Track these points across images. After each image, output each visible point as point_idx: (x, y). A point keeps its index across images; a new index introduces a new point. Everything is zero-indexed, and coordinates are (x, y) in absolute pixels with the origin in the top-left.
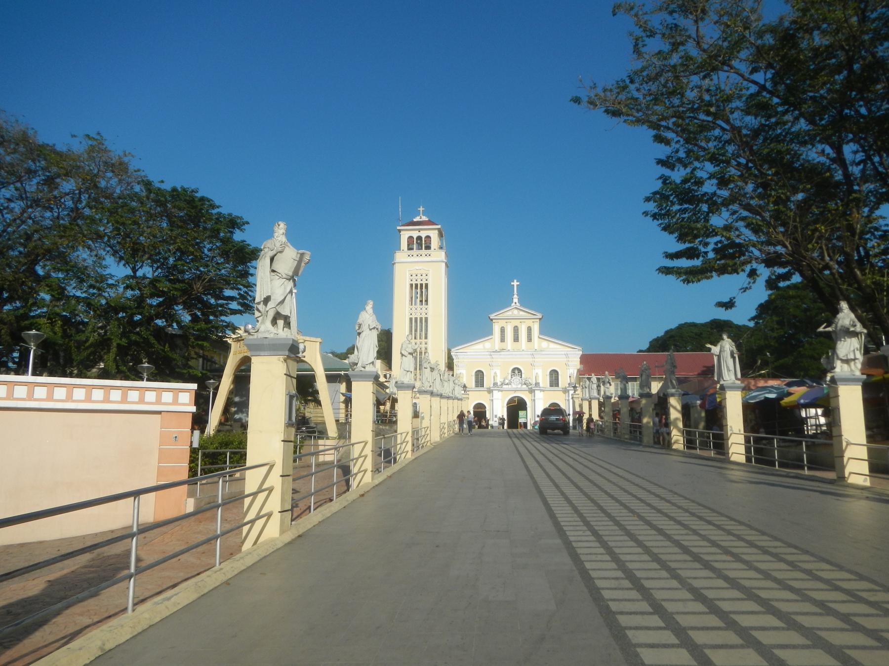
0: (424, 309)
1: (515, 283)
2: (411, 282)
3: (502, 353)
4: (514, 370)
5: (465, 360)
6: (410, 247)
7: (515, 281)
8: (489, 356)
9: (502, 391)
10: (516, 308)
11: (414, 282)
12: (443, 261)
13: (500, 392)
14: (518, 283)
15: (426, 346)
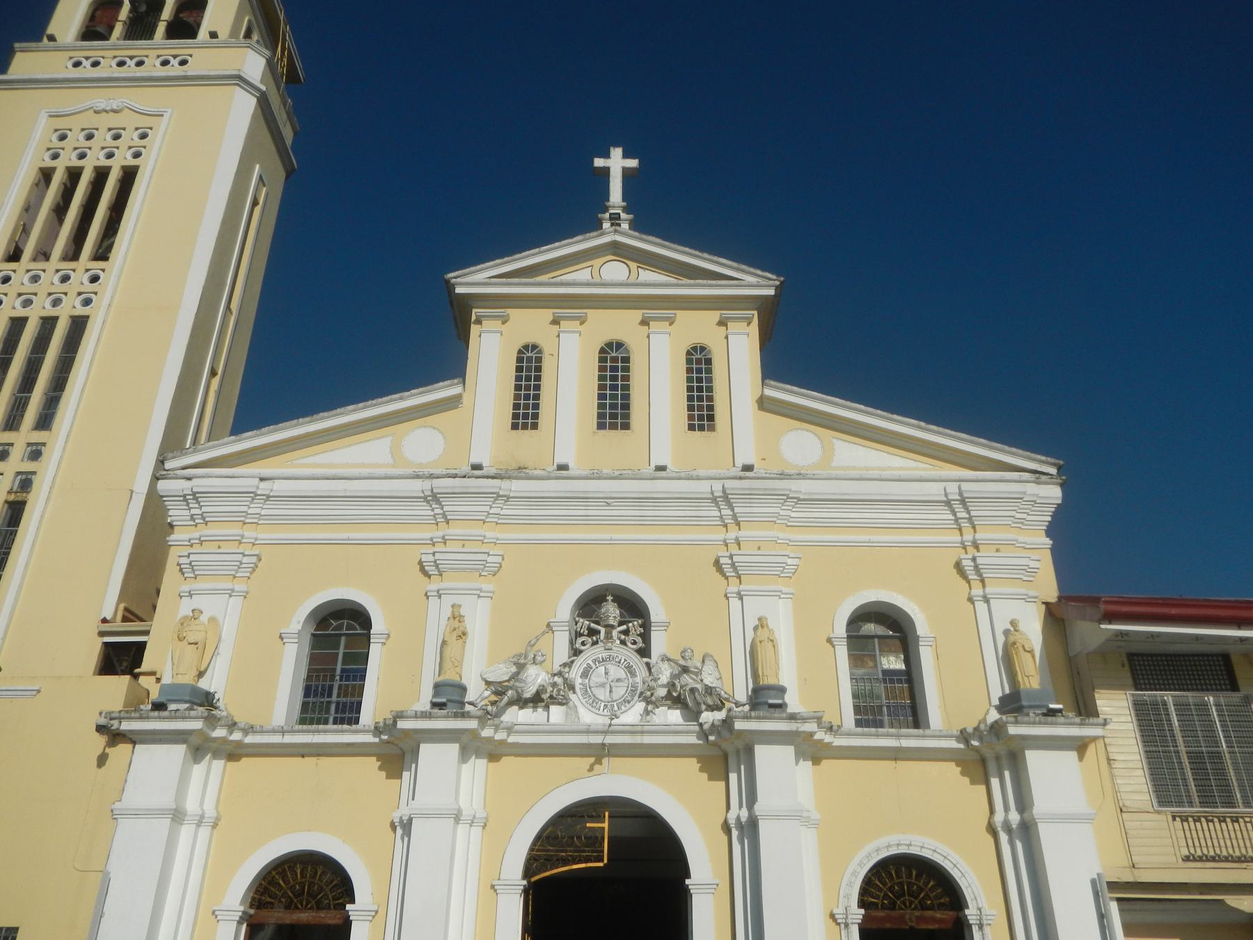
0: (80, 278)
1: (617, 163)
2: (49, 163)
3: (516, 486)
4: (590, 604)
5: (249, 533)
6: (100, 29)
7: (617, 153)
8: (424, 510)
9: (494, 753)
10: (618, 251)
11: (68, 159)
12: (240, 80)
13: (478, 766)
14: (633, 163)
15: (28, 466)
